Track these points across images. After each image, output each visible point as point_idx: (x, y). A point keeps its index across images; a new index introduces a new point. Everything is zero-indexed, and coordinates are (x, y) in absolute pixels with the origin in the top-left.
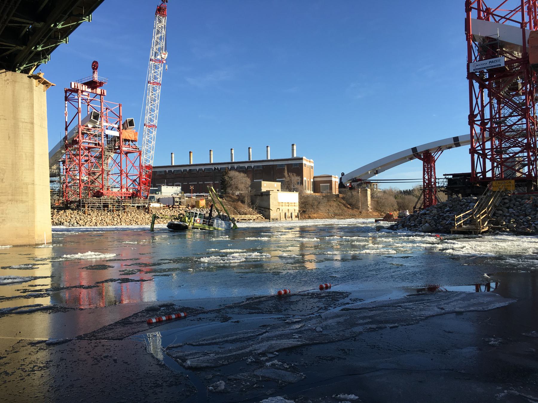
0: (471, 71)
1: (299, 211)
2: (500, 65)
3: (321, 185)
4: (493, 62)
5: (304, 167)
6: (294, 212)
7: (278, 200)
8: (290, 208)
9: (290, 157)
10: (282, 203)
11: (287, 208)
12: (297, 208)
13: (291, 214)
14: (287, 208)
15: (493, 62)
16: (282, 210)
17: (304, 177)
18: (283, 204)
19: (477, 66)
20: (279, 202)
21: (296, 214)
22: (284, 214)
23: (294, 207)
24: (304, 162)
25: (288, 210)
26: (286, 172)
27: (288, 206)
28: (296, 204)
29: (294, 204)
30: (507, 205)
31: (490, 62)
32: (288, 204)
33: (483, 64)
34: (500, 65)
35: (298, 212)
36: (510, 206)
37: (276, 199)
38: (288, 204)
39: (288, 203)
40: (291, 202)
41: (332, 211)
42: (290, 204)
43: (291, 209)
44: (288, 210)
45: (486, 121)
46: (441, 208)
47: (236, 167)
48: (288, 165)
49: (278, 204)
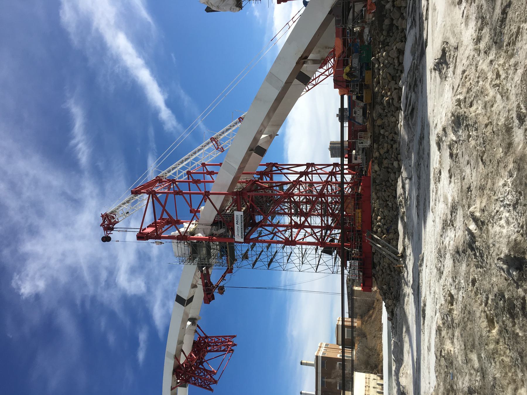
0: (242, 240)
1: (375, 374)
2: (241, 215)
3: (346, 338)
4: (237, 222)
5: (326, 355)
6: (376, 381)
9: (313, 369)
11: (371, 389)
12: (372, 376)
13: (378, 384)
14: (371, 389)
15: (237, 222)
17: (336, 357)
19: (238, 235)
21: (379, 378)
23: (371, 380)
24: (320, 354)
25: (374, 388)
26: (330, 380)
27: (369, 387)
28: (368, 377)
29: (367, 380)
30: (385, 231)
31: (237, 224)
32: (367, 387)
33: (238, 229)
34: (241, 215)
35: (376, 376)
36: (386, 229)
38: (367, 386)
39: (366, 387)
40: (365, 383)
41: (375, 333)
42: (367, 384)
43: (373, 384)
44: (374, 388)
45: (293, 224)
46: (385, 293)
48: (322, 378)
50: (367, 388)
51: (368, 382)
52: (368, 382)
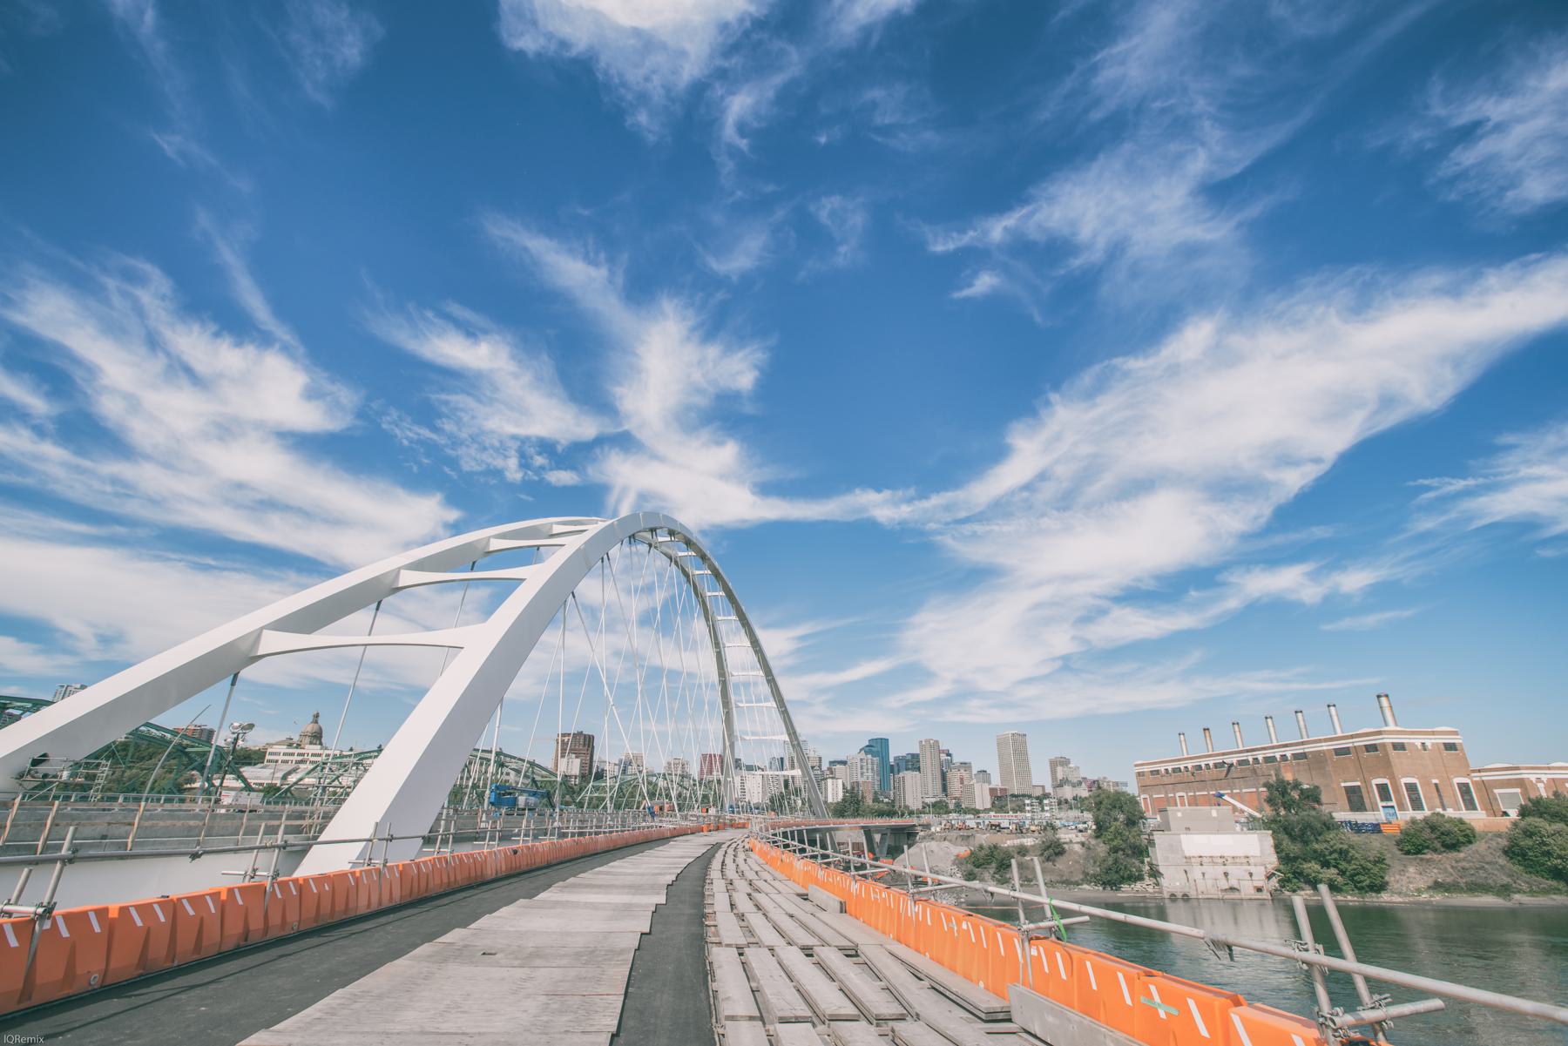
3: (1496, 791)
7: (1182, 850)
8: (1228, 869)
10: (1201, 857)
11: (1222, 869)
14: (1222, 869)
16: (1203, 874)
18: (1205, 860)
20: (1187, 854)
22: (1210, 882)
23: (1249, 868)
25: (1226, 874)
27: (1225, 865)
37: (1176, 848)
40: (1233, 855)
42: (1230, 860)
47: (1260, 758)
49: (1185, 860)
50: (1221, 860)
51: (1237, 860)
52: (1237, 860)
